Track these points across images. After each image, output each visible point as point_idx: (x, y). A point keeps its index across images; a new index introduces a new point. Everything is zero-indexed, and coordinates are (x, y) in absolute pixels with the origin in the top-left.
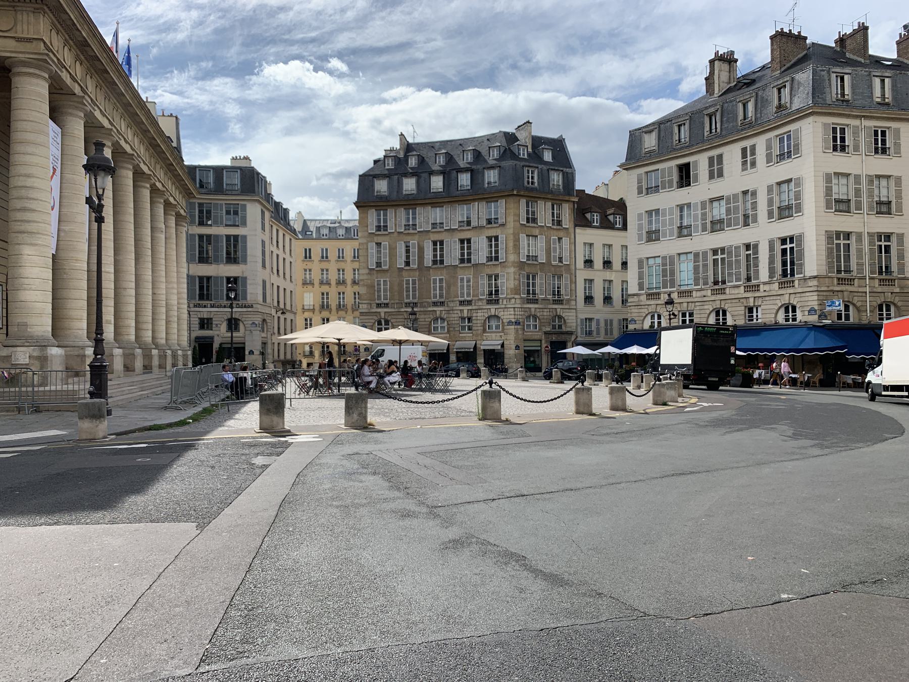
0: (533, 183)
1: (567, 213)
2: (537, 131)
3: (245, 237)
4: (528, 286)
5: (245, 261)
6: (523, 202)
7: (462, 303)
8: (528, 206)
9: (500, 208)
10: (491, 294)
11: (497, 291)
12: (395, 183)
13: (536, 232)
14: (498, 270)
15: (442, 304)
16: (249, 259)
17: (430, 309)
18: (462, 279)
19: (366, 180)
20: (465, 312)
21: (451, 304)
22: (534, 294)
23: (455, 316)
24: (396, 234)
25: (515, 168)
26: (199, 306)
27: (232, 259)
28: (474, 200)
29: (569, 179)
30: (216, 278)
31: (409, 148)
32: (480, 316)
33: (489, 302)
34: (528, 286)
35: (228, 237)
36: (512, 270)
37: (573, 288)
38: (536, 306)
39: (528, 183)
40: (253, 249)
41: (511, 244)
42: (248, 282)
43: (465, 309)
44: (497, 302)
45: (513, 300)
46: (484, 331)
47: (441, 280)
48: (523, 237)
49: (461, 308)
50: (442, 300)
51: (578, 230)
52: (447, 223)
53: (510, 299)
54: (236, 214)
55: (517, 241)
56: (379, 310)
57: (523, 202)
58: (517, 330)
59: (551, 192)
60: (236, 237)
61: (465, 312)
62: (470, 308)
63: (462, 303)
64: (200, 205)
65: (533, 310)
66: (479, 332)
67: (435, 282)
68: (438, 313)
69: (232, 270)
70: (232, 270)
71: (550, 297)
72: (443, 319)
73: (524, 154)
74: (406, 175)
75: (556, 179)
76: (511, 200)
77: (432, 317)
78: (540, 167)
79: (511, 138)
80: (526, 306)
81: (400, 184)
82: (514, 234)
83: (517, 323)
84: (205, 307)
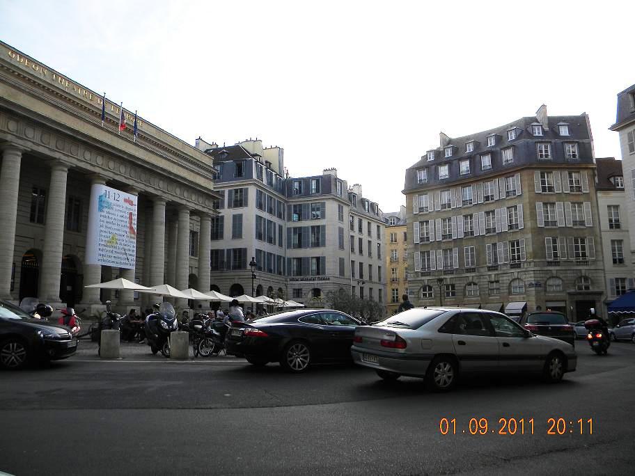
0: (547, 156)
1: (584, 180)
2: (552, 112)
3: (324, 227)
4: (518, 250)
5: (324, 245)
6: (537, 174)
7: (490, 269)
8: (543, 176)
9: (515, 182)
10: (514, 259)
11: (519, 258)
12: (433, 172)
13: (553, 199)
14: (518, 237)
15: (473, 270)
16: (327, 242)
17: (464, 275)
18: (467, 249)
19: (412, 173)
20: (493, 276)
21: (482, 270)
22: (584, 255)
23: (485, 280)
24: (434, 213)
25: (527, 145)
26: (293, 280)
27: (317, 244)
28: (495, 177)
29: (586, 150)
30: (305, 258)
31: (448, 142)
32: (505, 279)
33: (513, 266)
34: (518, 250)
35: (313, 227)
36: (529, 236)
37: (600, 250)
38: (558, 268)
39: (541, 156)
40: (331, 235)
41: (528, 212)
42: (326, 260)
43: (493, 273)
44: (518, 266)
45: (532, 264)
46: (510, 293)
47: (472, 249)
48: (539, 205)
49: (490, 273)
50: (473, 267)
51: (599, 194)
52: (474, 199)
53: (530, 262)
54: (320, 211)
55: (533, 209)
56: (423, 278)
57: (537, 174)
58: (537, 292)
59: (567, 162)
60: (318, 227)
61: (493, 276)
62: (496, 272)
63: (490, 269)
64: (295, 206)
65: (583, 272)
66: (506, 294)
67: (467, 251)
68: (471, 278)
69: (317, 252)
70: (317, 252)
71: (573, 259)
72: (475, 284)
73: (538, 132)
74: (441, 164)
75: (571, 150)
76: (525, 173)
77: (466, 282)
78: (553, 141)
79: (529, 122)
80: (546, 268)
81: (437, 171)
82: (530, 203)
83: (537, 285)
84: (297, 280)
